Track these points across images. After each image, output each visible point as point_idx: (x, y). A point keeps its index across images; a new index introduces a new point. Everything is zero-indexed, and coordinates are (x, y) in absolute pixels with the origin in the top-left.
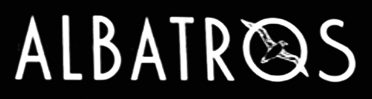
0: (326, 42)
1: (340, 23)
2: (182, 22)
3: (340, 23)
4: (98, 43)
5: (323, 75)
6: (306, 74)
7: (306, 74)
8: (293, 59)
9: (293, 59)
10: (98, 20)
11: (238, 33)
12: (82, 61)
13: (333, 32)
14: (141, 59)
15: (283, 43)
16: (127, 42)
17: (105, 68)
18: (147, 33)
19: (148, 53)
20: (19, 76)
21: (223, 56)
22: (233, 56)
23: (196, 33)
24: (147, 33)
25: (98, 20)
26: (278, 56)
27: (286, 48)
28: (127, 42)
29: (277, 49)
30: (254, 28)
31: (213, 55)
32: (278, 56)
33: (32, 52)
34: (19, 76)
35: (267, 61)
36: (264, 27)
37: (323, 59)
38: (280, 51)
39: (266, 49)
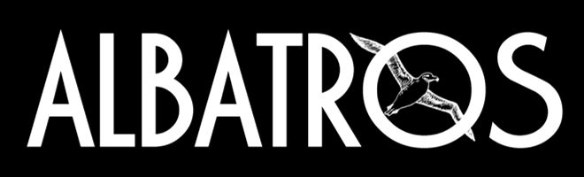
0: (180, 69)
1: (539, 41)
2: (279, 43)
3: (539, 41)
4: (151, 80)
5: (498, 135)
6: (472, 137)
7: (472, 137)
8: (448, 107)
9: (448, 107)
10: (151, 42)
11: (362, 60)
12: (128, 119)
13: (524, 58)
14: (215, 109)
15: (427, 78)
16: (197, 77)
17: (164, 123)
18: (228, 63)
19: (228, 97)
20: (36, 139)
21: (340, 103)
22: (351, 104)
23: (297, 58)
24: (228, 63)
25: (151, 42)
26: (419, 102)
27: (434, 88)
28: (197, 77)
29: (418, 89)
30: (385, 54)
31: (322, 102)
32: (419, 102)
33: (57, 99)
34: (36, 139)
35: (396, 111)
36: (402, 54)
37: (513, 107)
38: (424, 92)
39: (399, 89)
